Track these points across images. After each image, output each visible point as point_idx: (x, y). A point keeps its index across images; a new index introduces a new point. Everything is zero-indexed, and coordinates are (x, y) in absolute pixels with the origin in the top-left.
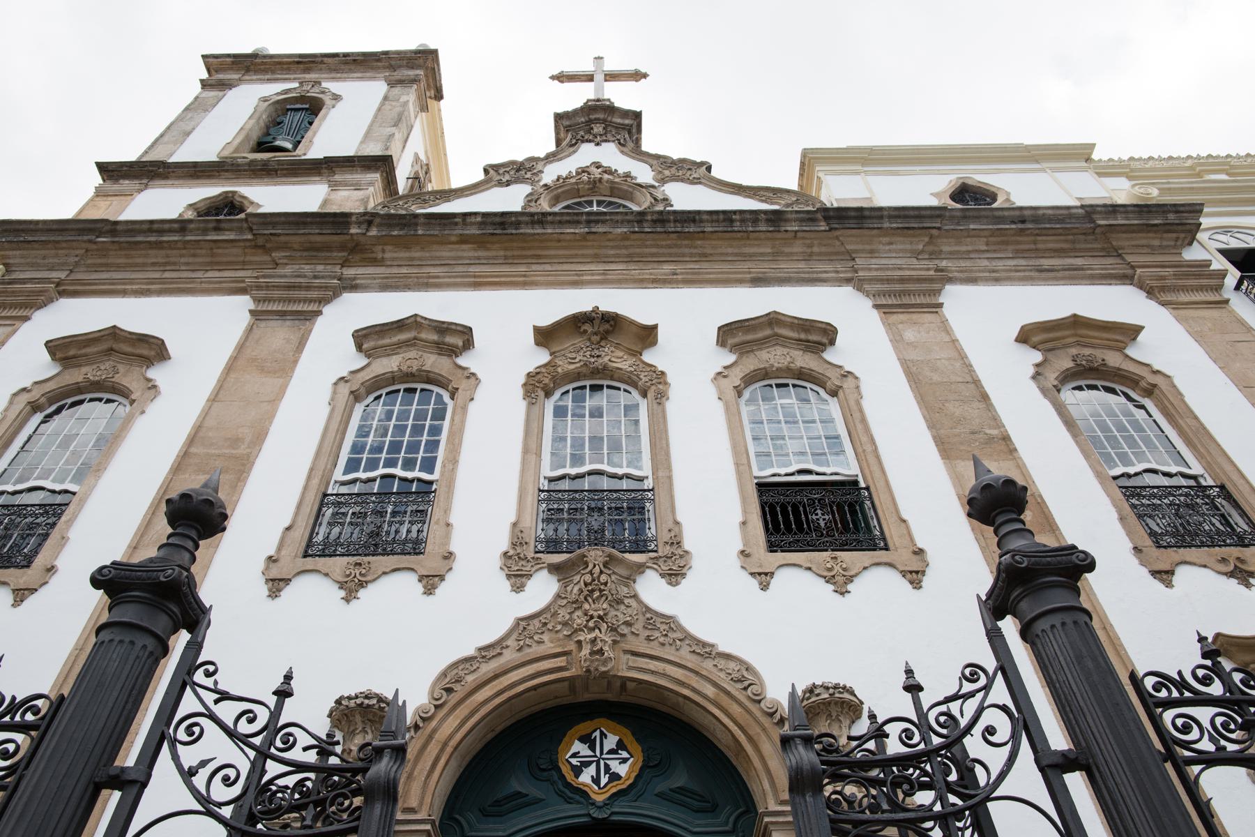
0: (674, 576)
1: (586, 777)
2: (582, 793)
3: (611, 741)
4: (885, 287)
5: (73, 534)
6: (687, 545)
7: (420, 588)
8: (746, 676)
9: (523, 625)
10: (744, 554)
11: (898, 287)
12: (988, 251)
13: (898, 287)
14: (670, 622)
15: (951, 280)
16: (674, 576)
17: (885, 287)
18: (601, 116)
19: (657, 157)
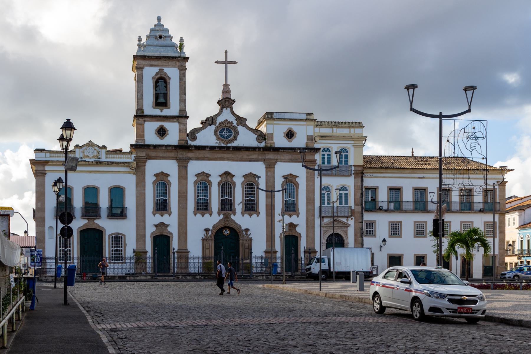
0: (234, 215)
1: (225, 233)
2: (225, 235)
3: (227, 230)
4: (268, 164)
5: (171, 207)
6: (236, 211)
7: (209, 216)
8: (240, 226)
9: (220, 220)
10: (241, 212)
11: (269, 164)
13: (269, 164)
14: (234, 221)
15: (278, 161)
16: (234, 215)
17: (268, 164)
18: (227, 99)
19: (238, 116)
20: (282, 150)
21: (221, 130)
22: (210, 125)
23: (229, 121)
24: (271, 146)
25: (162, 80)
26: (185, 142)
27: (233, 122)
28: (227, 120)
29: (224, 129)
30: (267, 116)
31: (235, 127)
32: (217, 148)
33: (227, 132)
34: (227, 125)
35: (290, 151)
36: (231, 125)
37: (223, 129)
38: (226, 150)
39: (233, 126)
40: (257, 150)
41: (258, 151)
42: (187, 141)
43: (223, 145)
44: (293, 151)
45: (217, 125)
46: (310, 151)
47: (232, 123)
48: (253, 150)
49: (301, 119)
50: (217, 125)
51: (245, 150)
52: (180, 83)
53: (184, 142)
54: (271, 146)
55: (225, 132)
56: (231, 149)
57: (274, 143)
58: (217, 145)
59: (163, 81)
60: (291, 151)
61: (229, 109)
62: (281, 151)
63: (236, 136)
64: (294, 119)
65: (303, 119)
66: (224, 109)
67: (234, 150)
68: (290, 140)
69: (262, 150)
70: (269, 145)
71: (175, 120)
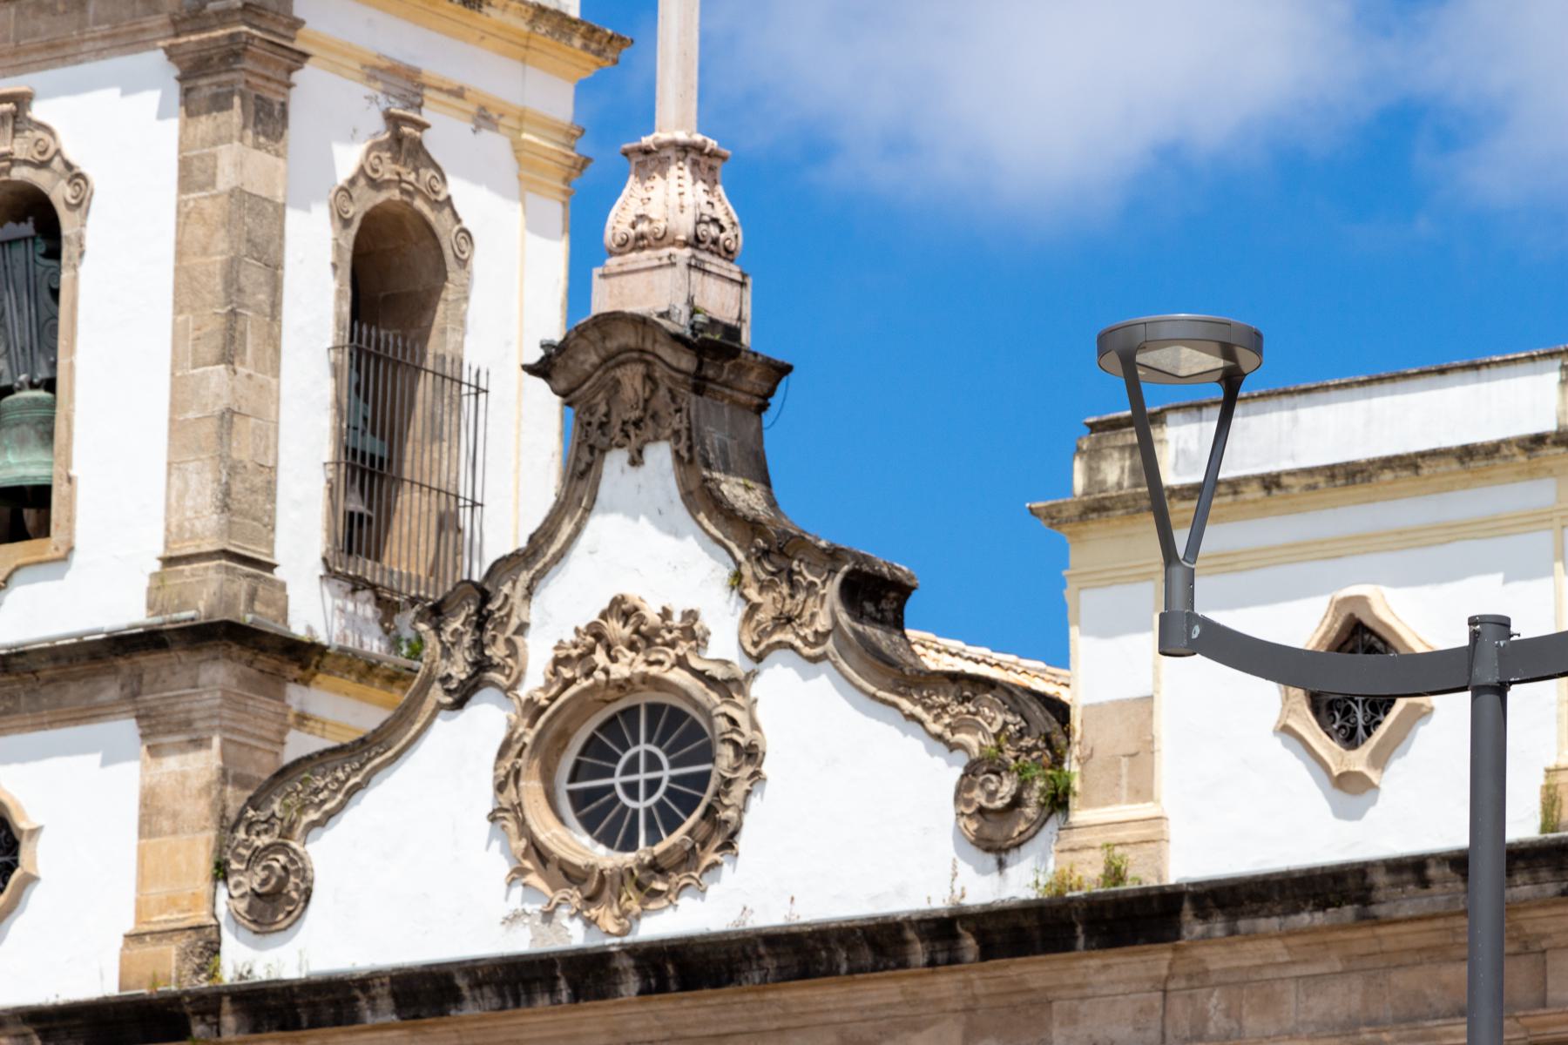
12: (1293, 963)
20: (1203, 914)
21: (591, 746)
22: (459, 704)
23: (652, 613)
24: (1115, 874)
25: (19, 219)
26: (184, 956)
27: (706, 621)
28: (622, 609)
29: (618, 729)
30: (1091, 471)
31: (728, 686)
32: (477, 984)
33: (653, 763)
34: (620, 671)
35: (1305, 919)
36: (681, 662)
37: (609, 726)
38: (576, 997)
39: (699, 674)
40: (918, 952)
41: (932, 963)
42: (213, 948)
43: (573, 935)
44: (1349, 911)
45: (523, 692)
46: (1551, 889)
47: (691, 630)
48: (867, 956)
49: (1467, 453)
50: (534, 681)
51: (786, 976)
52: (184, 217)
53: (170, 952)
54: (1115, 874)
55: (632, 767)
56: (631, 985)
57: (1153, 837)
58: (520, 942)
59: (27, 228)
60: (1319, 918)
61: (660, 455)
62: (1199, 929)
63: (737, 791)
64: (1389, 463)
65: (1491, 451)
66: (615, 463)
67: (662, 988)
68: (1357, 760)
69: (969, 943)
70: (1088, 876)
71: (111, 690)
